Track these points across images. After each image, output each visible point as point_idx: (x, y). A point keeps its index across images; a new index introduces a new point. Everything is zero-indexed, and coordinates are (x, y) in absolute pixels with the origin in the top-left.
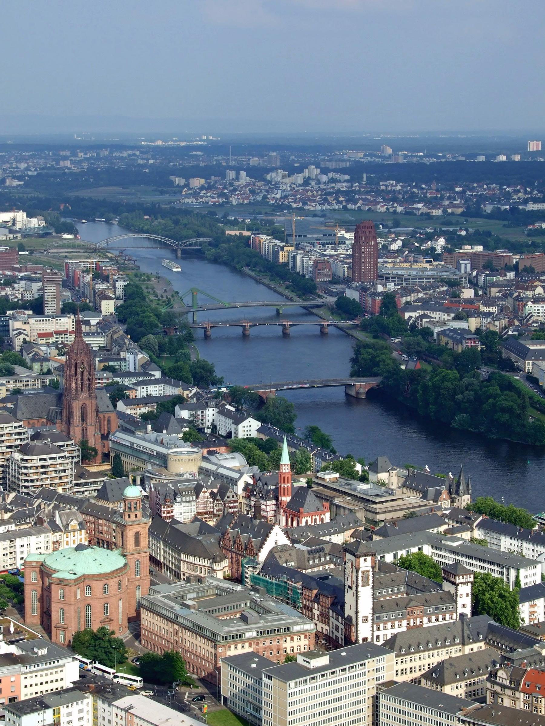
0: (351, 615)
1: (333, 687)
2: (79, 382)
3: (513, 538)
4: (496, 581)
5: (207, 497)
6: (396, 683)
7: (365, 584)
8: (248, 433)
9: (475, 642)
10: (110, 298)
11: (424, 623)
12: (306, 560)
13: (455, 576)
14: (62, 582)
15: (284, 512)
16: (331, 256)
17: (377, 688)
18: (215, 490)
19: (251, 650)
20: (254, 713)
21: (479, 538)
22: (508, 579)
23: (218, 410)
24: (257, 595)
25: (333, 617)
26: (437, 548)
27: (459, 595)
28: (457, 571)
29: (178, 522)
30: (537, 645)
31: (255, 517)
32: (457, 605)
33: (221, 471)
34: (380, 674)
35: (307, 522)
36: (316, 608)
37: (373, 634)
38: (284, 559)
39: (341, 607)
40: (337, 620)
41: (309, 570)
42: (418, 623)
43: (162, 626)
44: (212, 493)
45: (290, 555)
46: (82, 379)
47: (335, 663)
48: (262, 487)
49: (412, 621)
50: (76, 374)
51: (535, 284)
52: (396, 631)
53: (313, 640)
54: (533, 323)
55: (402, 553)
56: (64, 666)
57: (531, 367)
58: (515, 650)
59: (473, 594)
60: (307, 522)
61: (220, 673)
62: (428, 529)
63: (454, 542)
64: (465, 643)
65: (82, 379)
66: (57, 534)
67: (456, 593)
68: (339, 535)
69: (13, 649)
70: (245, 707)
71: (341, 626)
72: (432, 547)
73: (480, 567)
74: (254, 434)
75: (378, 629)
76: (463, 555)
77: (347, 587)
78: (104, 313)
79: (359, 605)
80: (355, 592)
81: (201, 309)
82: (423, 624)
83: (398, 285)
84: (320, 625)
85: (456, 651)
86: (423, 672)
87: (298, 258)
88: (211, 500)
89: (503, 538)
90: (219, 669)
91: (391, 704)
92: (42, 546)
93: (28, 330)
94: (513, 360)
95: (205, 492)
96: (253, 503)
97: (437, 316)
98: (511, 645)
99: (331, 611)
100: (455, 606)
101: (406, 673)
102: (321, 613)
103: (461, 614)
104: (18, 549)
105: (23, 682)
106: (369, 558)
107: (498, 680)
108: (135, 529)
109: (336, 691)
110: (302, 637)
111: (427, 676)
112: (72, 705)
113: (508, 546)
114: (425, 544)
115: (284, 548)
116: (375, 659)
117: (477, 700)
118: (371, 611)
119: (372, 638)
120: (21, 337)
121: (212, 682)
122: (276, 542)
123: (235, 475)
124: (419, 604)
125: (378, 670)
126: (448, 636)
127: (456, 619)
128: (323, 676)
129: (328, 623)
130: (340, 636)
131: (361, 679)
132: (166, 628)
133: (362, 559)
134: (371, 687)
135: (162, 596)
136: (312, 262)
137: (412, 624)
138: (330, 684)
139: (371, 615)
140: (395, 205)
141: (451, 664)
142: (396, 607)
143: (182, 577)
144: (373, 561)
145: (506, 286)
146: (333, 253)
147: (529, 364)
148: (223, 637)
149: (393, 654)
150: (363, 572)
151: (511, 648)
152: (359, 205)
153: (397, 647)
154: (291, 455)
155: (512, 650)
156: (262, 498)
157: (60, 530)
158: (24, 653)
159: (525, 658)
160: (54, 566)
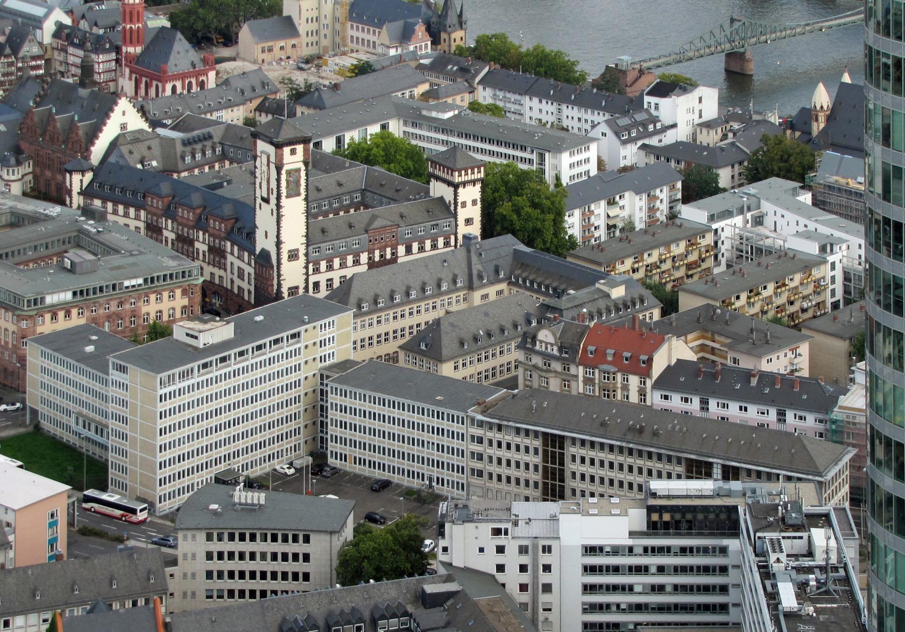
0: (267, 248)
1: (242, 379)
3: (544, 101)
4: (525, 175)
6: (355, 363)
9: (491, 283)
11: (399, 255)
12: (178, 157)
13: (452, 171)
15: (131, 72)
17: (322, 376)
19: (82, 321)
21: (485, 103)
22: (543, 172)
24: (92, 222)
25: (232, 253)
26: (414, 125)
27: (459, 204)
28: (455, 161)
30: (602, 281)
32: (456, 221)
34: (327, 350)
35: (174, 89)
36: (201, 239)
37: (307, 281)
38: (137, 156)
39: (248, 234)
40: (240, 258)
41: (184, 174)
42: (388, 256)
45: (149, 148)
47: (243, 335)
48: (88, 29)
49: (377, 253)
52: (349, 272)
53: (198, 298)
55: (352, 136)
58: (563, 291)
59: (483, 200)
60: (174, 89)
61: (24, 366)
62: (394, 92)
63: (445, 112)
64: (475, 285)
67: (455, 199)
68: (235, 109)
71: (249, 270)
72: (405, 124)
73: (492, 153)
75: (317, 271)
76: (460, 135)
79: (282, 231)
80: (275, 208)
82: (397, 257)
84: (208, 269)
85: (458, 301)
86: (401, 342)
89: (526, 100)
90: (22, 360)
91: (348, 402)
98: (554, 285)
99: (229, 244)
100: (454, 223)
101: (370, 344)
102: (211, 249)
103: (464, 237)
107: (537, 347)
109: (245, 386)
110: (178, 292)
113: (535, 114)
114: (390, 118)
115: (138, 137)
116: (318, 324)
117: (500, 384)
118: (304, 240)
119: (306, 288)
121: (6, 383)
122: (123, 127)
124: (390, 223)
125: (322, 343)
126: (443, 276)
127: (456, 246)
128: (223, 360)
129: (225, 264)
130: (247, 287)
131: (293, 361)
134: (310, 374)
137: (377, 259)
139: (304, 247)
141: (452, 325)
142: (349, 231)
148: (29, 301)
151: (555, 290)
153: (353, 299)
155: (558, 294)
159: (581, 305)
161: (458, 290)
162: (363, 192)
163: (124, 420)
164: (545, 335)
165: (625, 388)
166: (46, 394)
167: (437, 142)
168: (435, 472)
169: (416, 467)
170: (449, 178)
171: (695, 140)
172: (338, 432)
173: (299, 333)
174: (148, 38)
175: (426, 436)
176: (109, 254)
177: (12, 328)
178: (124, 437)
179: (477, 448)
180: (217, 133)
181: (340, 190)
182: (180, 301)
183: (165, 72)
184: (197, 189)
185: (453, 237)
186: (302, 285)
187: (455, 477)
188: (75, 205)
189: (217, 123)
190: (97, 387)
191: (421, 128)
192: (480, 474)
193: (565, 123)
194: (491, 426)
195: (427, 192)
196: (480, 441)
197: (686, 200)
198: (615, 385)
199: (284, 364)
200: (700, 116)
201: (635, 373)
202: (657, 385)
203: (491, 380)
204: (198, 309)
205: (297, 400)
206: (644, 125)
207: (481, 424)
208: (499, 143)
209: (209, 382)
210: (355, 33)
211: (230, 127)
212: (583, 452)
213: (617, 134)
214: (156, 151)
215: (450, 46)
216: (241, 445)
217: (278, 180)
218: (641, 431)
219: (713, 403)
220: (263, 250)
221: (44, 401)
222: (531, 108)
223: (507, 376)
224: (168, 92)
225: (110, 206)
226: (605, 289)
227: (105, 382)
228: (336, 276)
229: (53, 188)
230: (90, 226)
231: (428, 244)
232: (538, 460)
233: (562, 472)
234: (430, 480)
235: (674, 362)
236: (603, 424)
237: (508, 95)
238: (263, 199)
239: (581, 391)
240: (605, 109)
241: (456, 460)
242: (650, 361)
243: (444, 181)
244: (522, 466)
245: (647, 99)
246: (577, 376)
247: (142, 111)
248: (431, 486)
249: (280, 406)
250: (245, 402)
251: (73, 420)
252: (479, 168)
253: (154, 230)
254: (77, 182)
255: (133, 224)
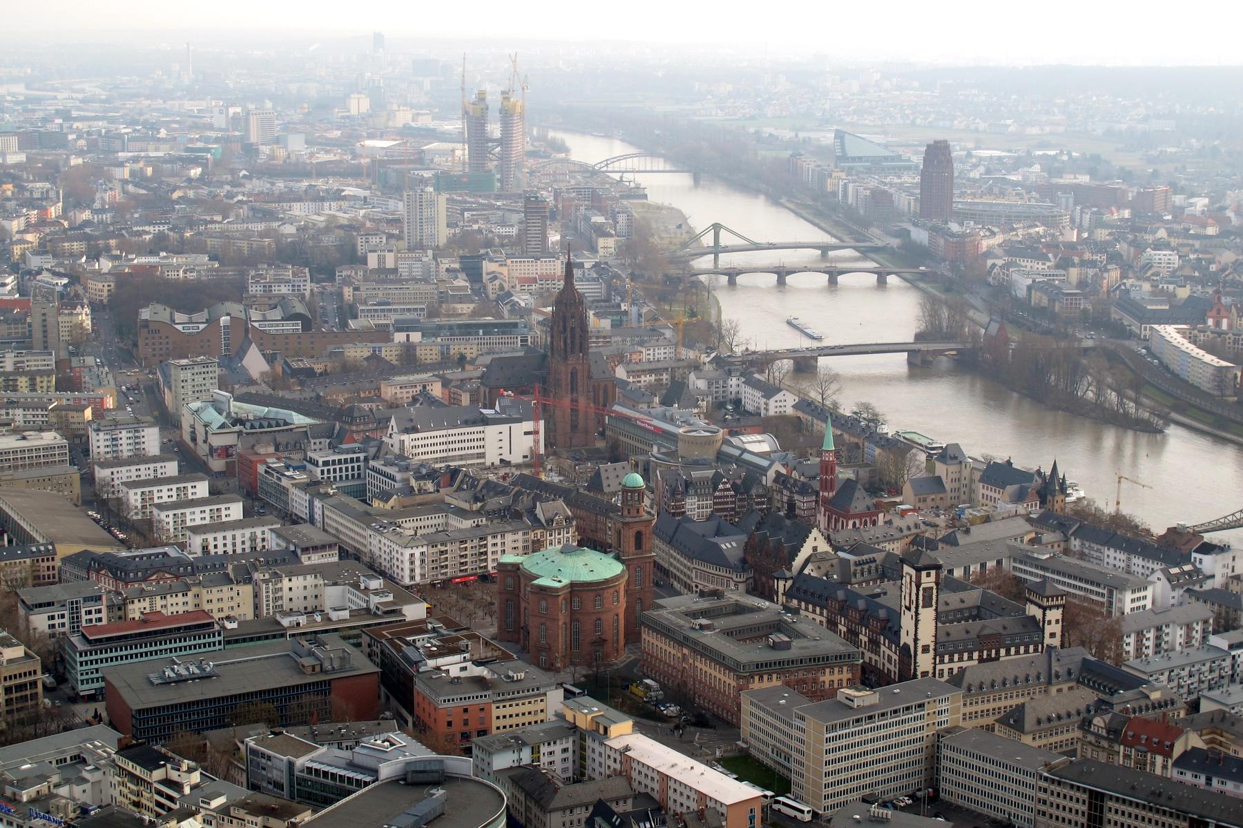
1: (883, 732)
2: (569, 341)
5: (728, 490)
7: (927, 604)
8: (782, 409)
9: (1066, 681)
10: (609, 235)
14: (543, 589)
16: (891, 185)
18: (739, 482)
20: (782, 760)
23: (743, 379)
26: (1021, 562)
29: (691, 520)
31: (788, 516)
33: (746, 456)
34: (943, 718)
37: (935, 668)
40: (890, 648)
42: (993, 656)
43: (669, 649)
44: (735, 487)
46: (573, 337)
49: (985, 652)
50: (565, 330)
51: (1157, 225)
54: (1152, 275)
56: (545, 694)
57: (1148, 333)
58: (1116, 691)
60: (854, 524)
61: (739, 710)
65: (573, 337)
66: (539, 532)
67: (1044, 618)
69: (482, 671)
70: (770, 753)
71: (895, 657)
73: (1075, 587)
74: (790, 411)
75: (942, 662)
76: (1053, 572)
77: (903, 608)
78: (601, 252)
81: (727, 250)
83: (979, 224)
84: (868, 655)
86: (997, 717)
87: (851, 186)
88: (732, 493)
90: (739, 706)
92: (520, 544)
93: (506, 273)
94: (1126, 323)
95: (725, 483)
96: (785, 499)
97: (1029, 265)
98: (1110, 686)
102: (870, 640)
104: (490, 549)
105: (495, 712)
106: (933, 573)
108: (637, 528)
110: (845, 669)
111: (1003, 721)
112: (555, 743)
113: (1111, 561)
117: (1064, 753)
118: (933, 639)
120: (497, 282)
122: (815, 549)
123: (765, 463)
125: (940, 713)
128: (870, 718)
130: (894, 669)
131: (919, 723)
132: (673, 652)
133: (924, 573)
135: (670, 613)
136: (868, 192)
137: (985, 657)
138: (879, 728)
140: (977, 121)
143: (694, 589)
144: (937, 576)
145: (1118, 227)
146: (896, 180)
147: (1145, 330)
149: (961, 692)
150: (925, 589)
151: (1110, 689)
152: (930, 119)
153: (965, 684)
154: (836, 437)
156: (797, 493)
157: (542, 526)
158: (496, 676)
159: (1127, 702)
160: (534, 571)
161: (1040, 684)
162: (978, 608)
163: (802, 753)
164: (1098, 721)
165: (1153, 764)
166: (753, 731)
167: (1037, 575)
168: (1013, 810)
169: (1000, 805)
170: (1040, 602)
171: (1227, 588)
172: (947, 775)
173: (924, 704)
174: (837, 486)
175: (1007, 784)
176: (799, 637)
177: (733, 684)
178: (802, 764)
179: (1042, 795)
180: (879, 557)
181: (962, 606)
182: (846, 675)
183: (849, 511)
184: (861, 597)
185: (1040, 646)
186: (931, 671)
187: (1027, 814)
188: (780, 602)
189: (881, 551)
190: (786, 729)
191: (1025, 565)
192: (1044, 814)
193: (1133, 568)
194: (1053, 781)
195: (1024, 611)
196: (1045, 791)
197: (1215, 632)
198: (1146, 761)
199: (913, 725)
200: (1233, 571)
201: (1160, 754)
202: (1177, 764)
203: (1059, 750)
204: (858, 681)
205: (920, 750)
206: (1189, 573)
207: (1046, 779)
208: (1081, 580)
209: (860, 732)
210: (985, 492)
211: (889, 555)
212: (1117, 806)
213: (1169, 580)
214: (837, 568)
215: (1053, 505)
216: (880, 777)
217: (917, 595)
218: (1160, 795)
219: (1215, 781)
220: (905, 644)
221: (751, 735)
222: (1108, 556)
223: (1070, 748)
224: (850, 526)
225: (803, 604)
226: (1146, 692)
227: (791, 726)
228: (955, 666)
229: (767, 589)
230: (788, 617)
231: (1022, 649)
232: (1085, 808)
233: (1101, 818)
234: (1009, 815)
235: (1189, 748)
236: (1133, 788)
237: (1092, 545)
238: (906, 607)
239: (1121, 762)
240: (1162, 560)
241: (1027, 803)
242: (1172, 746)
243: (1036, 604)
244: (1074, 811)
245: (1194, 555)
246: (1119, 753)
247: (828, 539)
248: (1009, 818)
249: (908, 753)
250: (884, 749)
251: (770, 749)
252: (1062, 596)
253: (832, 625)
254: (781, 586)
255: (818, 618)
